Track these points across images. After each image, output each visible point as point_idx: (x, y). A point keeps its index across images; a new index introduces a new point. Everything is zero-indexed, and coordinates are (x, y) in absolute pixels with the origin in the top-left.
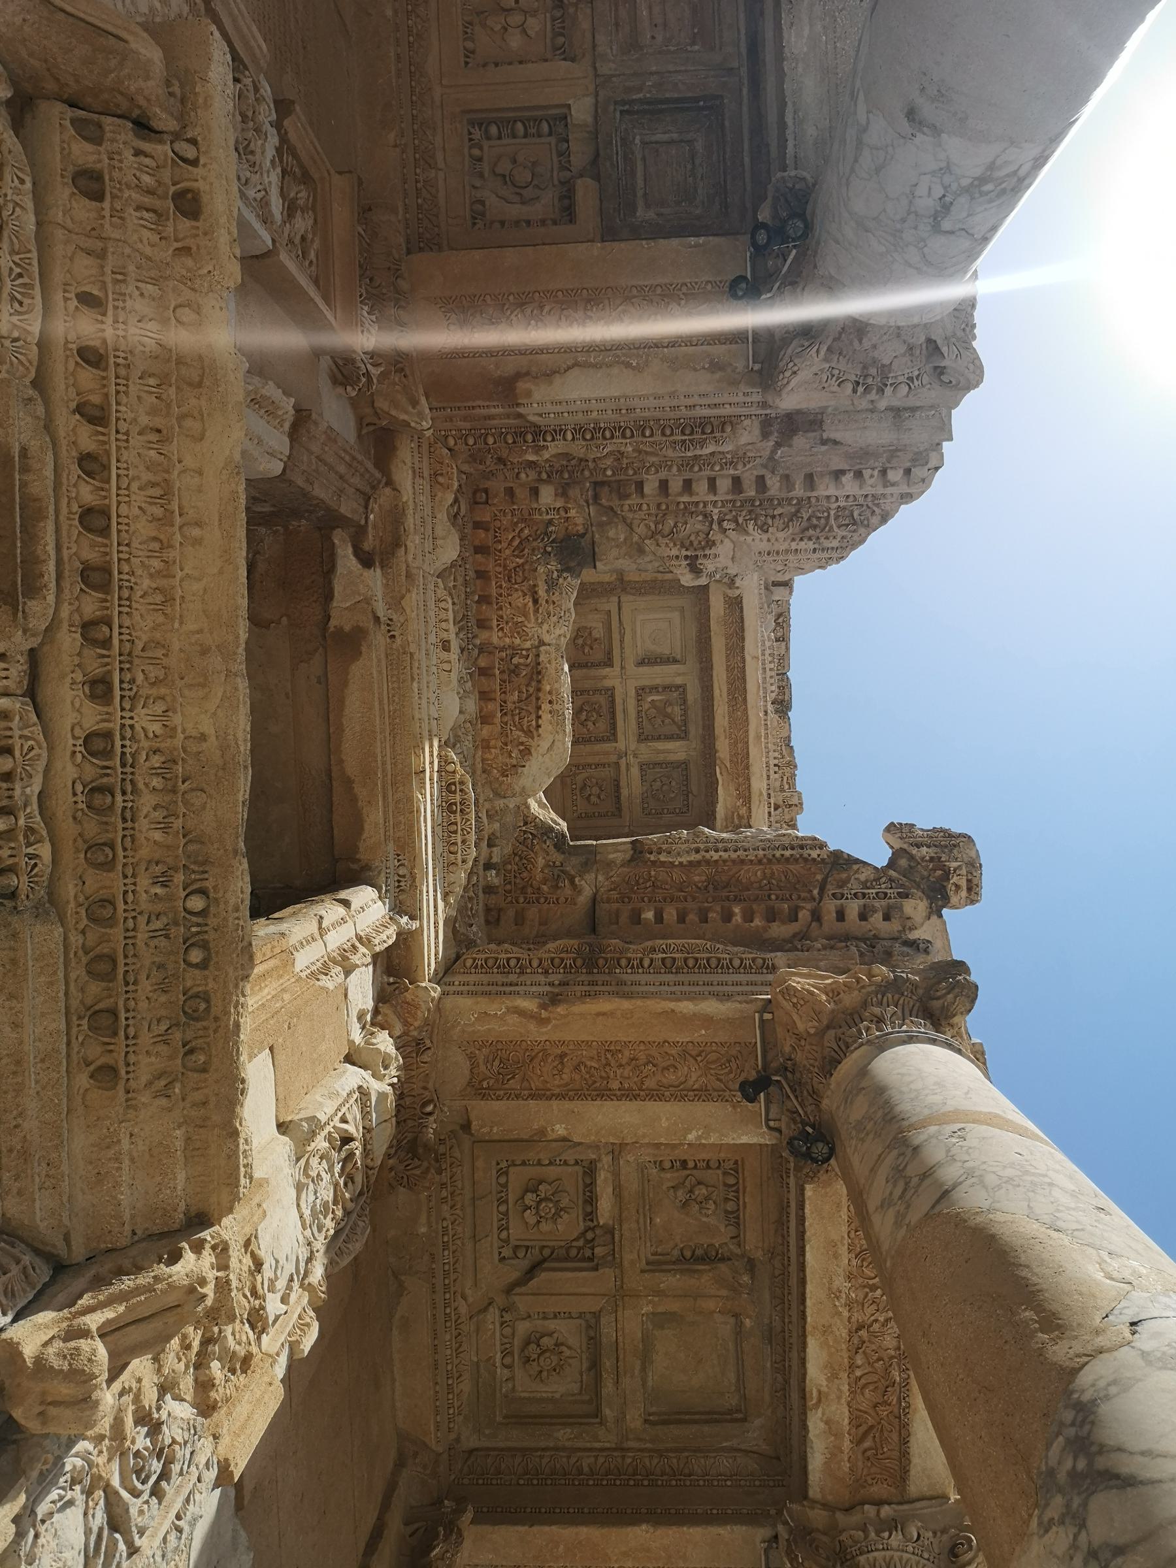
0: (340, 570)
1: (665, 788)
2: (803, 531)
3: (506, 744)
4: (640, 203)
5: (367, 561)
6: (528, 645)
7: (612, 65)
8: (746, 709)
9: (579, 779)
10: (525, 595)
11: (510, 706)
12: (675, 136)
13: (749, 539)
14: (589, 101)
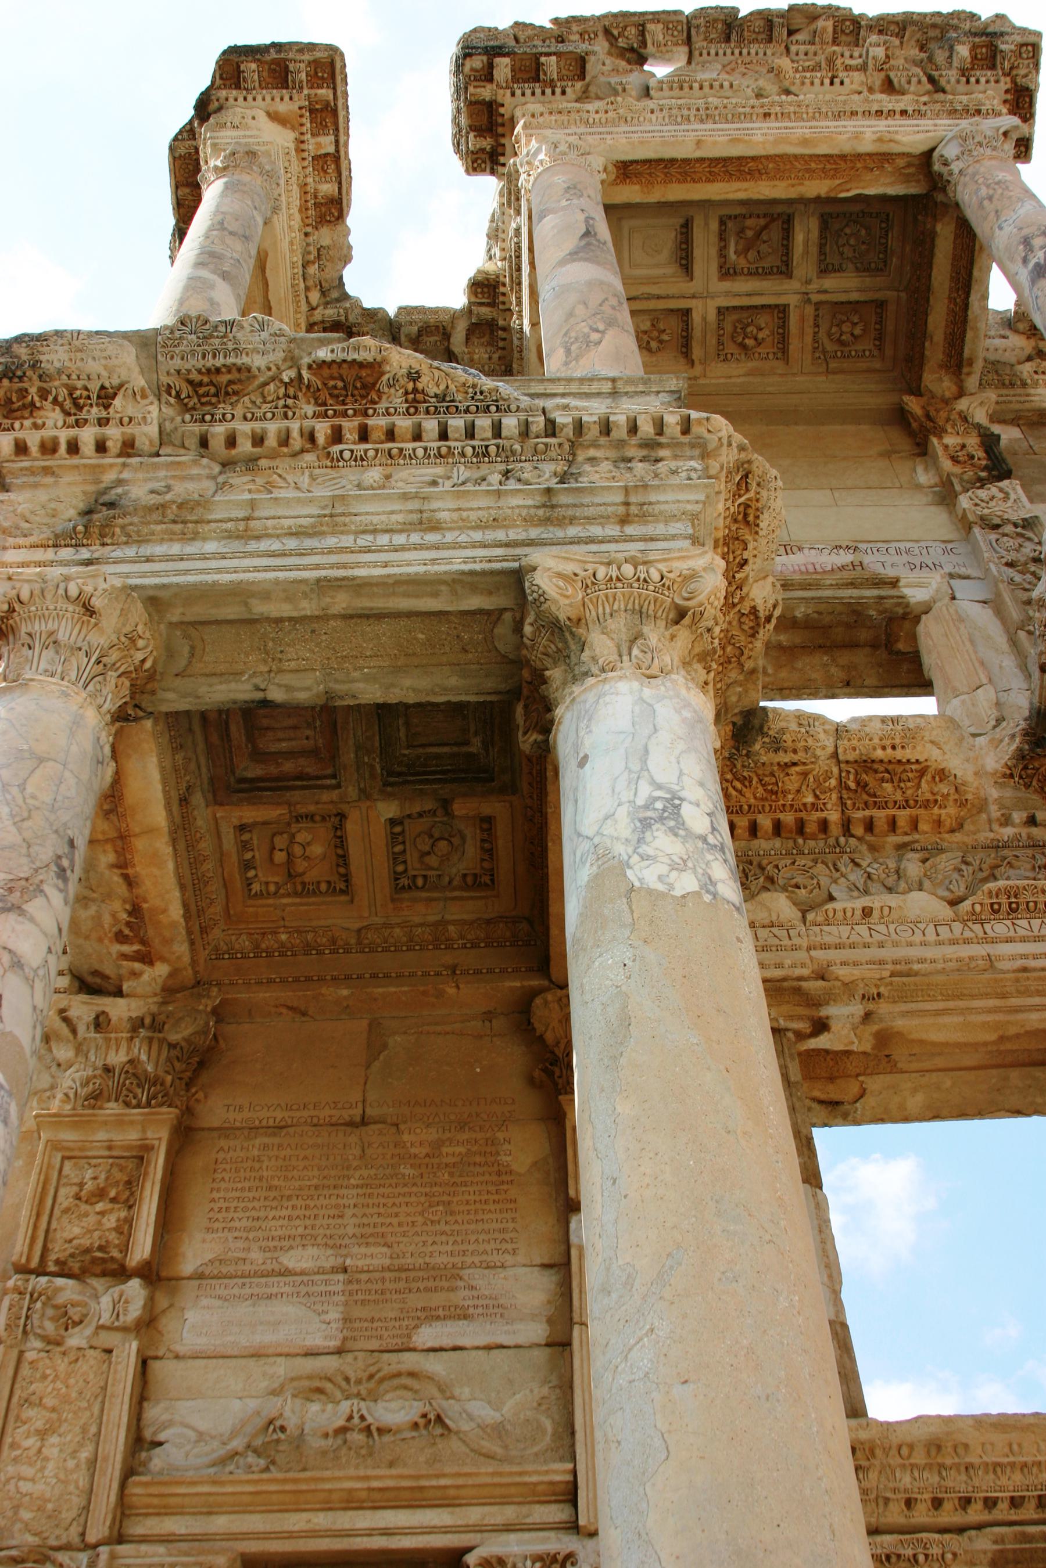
0: (827, 1046)
1: (852, 242)
2: (747, 523)
3: (936, 801)
4: (464, 749)
5: (821, 1026)
6: (835, 770)
7: (350, 789)
8: (767, 157)
9: (830, 347)
10: (787, 774)
11: (899, 796)
12: (401, 721)
13: (752, 574)
14: (381, 805)
